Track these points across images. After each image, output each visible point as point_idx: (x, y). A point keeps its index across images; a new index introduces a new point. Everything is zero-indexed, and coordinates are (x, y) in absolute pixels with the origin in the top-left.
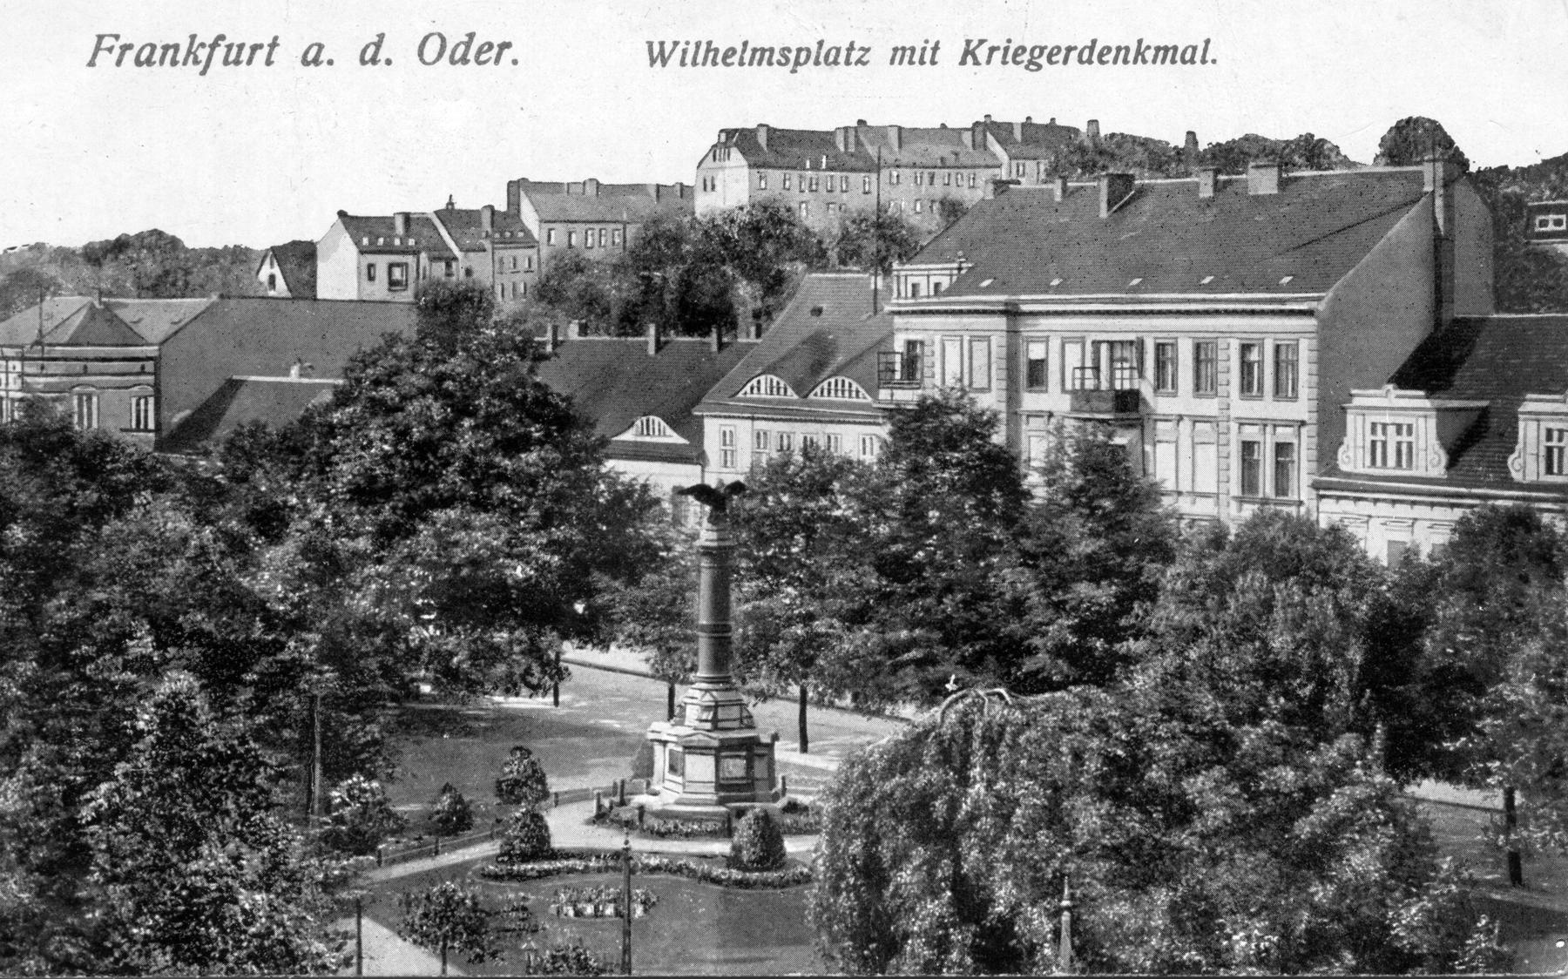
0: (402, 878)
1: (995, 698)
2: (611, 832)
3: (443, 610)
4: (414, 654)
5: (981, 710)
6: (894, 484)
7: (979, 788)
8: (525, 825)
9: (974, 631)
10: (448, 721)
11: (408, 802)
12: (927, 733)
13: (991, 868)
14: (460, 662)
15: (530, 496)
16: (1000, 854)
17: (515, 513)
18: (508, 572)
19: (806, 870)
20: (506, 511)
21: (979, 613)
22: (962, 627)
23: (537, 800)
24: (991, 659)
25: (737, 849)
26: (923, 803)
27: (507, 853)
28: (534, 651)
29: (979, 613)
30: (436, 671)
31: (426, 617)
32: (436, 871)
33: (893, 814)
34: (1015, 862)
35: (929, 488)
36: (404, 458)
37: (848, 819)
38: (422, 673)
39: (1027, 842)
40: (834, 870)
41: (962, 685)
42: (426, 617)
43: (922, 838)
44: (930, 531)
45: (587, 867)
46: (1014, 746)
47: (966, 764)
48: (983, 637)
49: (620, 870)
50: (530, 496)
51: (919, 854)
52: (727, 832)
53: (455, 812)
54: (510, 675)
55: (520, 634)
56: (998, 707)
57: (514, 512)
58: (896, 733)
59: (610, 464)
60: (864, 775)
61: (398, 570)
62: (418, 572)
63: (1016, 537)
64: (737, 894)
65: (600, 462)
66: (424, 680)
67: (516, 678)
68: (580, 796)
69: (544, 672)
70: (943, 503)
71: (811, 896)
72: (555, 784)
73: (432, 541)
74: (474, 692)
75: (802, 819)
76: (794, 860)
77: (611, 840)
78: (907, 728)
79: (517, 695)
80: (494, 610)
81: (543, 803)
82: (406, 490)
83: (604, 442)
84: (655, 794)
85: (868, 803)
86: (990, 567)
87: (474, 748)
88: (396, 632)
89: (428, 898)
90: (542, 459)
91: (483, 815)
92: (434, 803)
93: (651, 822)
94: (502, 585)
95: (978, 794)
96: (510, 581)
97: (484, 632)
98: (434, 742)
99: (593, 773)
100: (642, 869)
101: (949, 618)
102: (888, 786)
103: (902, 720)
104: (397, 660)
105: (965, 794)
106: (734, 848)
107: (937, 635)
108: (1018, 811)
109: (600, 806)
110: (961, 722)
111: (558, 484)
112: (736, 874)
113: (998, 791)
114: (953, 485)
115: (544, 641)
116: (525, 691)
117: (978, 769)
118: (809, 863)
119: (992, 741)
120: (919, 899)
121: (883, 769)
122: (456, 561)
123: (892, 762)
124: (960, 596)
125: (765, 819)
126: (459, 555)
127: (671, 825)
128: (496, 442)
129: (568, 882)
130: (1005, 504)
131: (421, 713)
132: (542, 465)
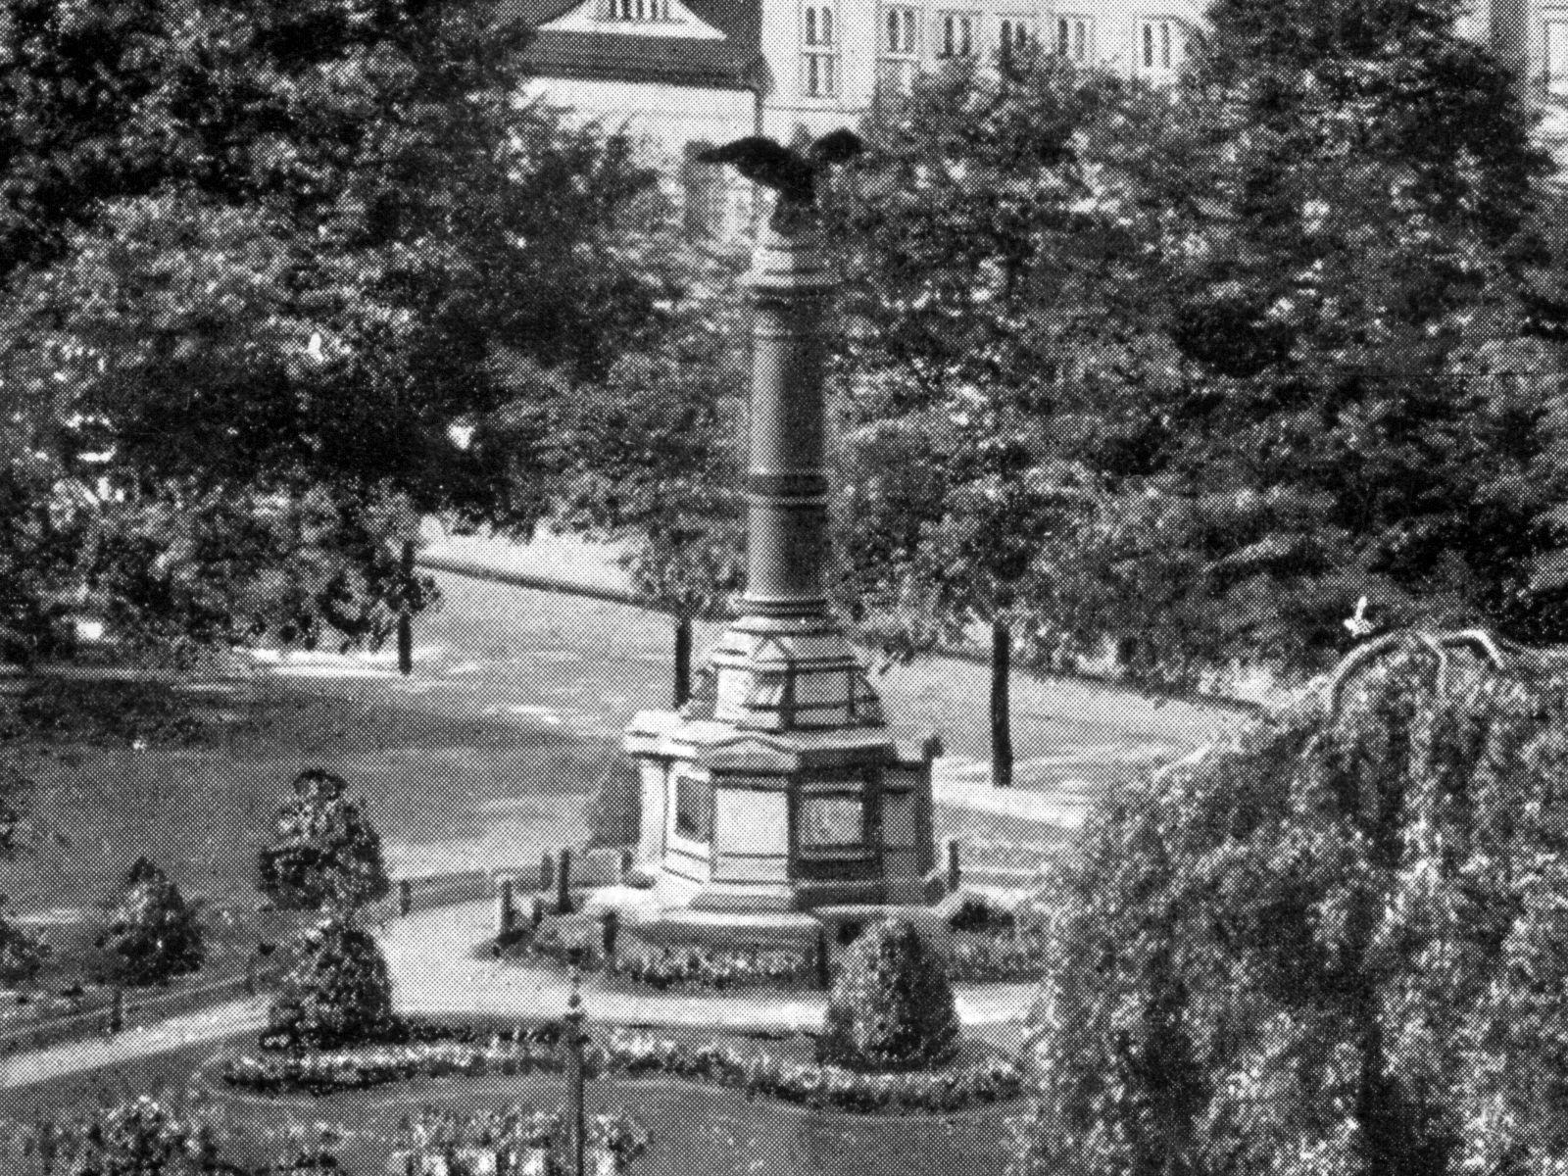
0: (34, 1088)
1: (1464, 654)
2: (539, 975)
3: (131, 440)
4: (60, 548)
5: (1429, 683)
6: (1220, 137)
7: (1424, 871)
8: (329, 960)
9: (1412, 492)
10: (145, 708)
11: (48, 903)
12: (1299, 737)
13: (1453, 1063)
14: (172, 567)
15: (343, 165)
16: (1475, 1029)
17: (304, 205)
18: (288, 348)
19: (1007, 1069)
20: (284, 201)
21: (1424, 448)
22: (1384, 482)
23: (359, 899)
24: (1453, 557)
25: (841, 1017)
26: (1291, 905)
27: (287, 1028)
28: (352, 539)
29: (1424, 448)
30: (115, 588)
31: (91, 457)
32: (116, 1069)
33: (1218, 933)
34: (1512, 1048)
35: (1305, 147)
36: (37, 74)
37: (1108, 945)
38: (82, 592)
39: (1541, 1000)
40: (1076, 1068)
41: (1385, 621)
42: (91, 457)
43: (1288, 990)
44: (1307, 250)
45: (478, 1061)
46: (1509, 769)
47: (1393, 814)
48: (1434, 507)
49: (559, 1068)
50: (343, 165)
51: (1281, 1028)
52: (818, 976)
53: (161, 928)
54: (293, 597)
55: (317, 497)
56: (1470, 676)
57: (303, 204)
58: (1225, 738)
59: (534, 90)
60: (1147, 839)
61: (23, 344)
62: (72, 348)
63: (1513, 264)
64: (842, 1127)
65: (510, 84)
66: (87, 610)
67: (308, 604)
68: (463, 890)
69: (375, 591)
70: (1338, 183)
71: (1020, 1130)
72: (402, 860)
73: (105, 274)
74: (207, 639)
75: (999, 945)
76: (977, 1045)
77: (535, 995)
78: (1250, 726)
79: (311, 645)
80: (255, 440)
81: (373, 907)
82: (43, 151)
83: (519, 36)
84: (644, 884)
85: (1157, 905)
86: (1451, 336)
87: (205, 774)
88: (19, 495)
89: (95, 1135)
90: (372, 77)
91: (229, 936)
92: (110, 905)
93: (644, 955)
94: (274, 381)
95: (1422, 884)
96: (293, 371)
97: (230, 492)
98: (111, 759)
99: (494, 833)
100: (613, 1066)
101: (1353, 460)
102: (1205, 866)
103: (1240, 705)
104: (22, 561)
105: (1392, 885)
106: (834, 1015)
107: (1323, 502)
108: (1520, 926)
109: (509, 914)
110: (1381, 710)
111: (410, 138)
112: (839, 1078)
113: (1472, 878)
114: (1362, 142)
115: (375, 517)
116: (329, 635)
117: (1423, 825)
118: (1015, 1050)
119: (1456, 756)
120: (1281, 1138)
121: (1194, 824)
122: (163, 322)
123: (1216, 806)
124: (1378, 408)
125: (910, 945)
126: (171, 309)
127: (681, 960)
128: (261, 36)
129: (432, 1097)
130: (1488, 187)
131: (80, 689)
132: (371, 90)
